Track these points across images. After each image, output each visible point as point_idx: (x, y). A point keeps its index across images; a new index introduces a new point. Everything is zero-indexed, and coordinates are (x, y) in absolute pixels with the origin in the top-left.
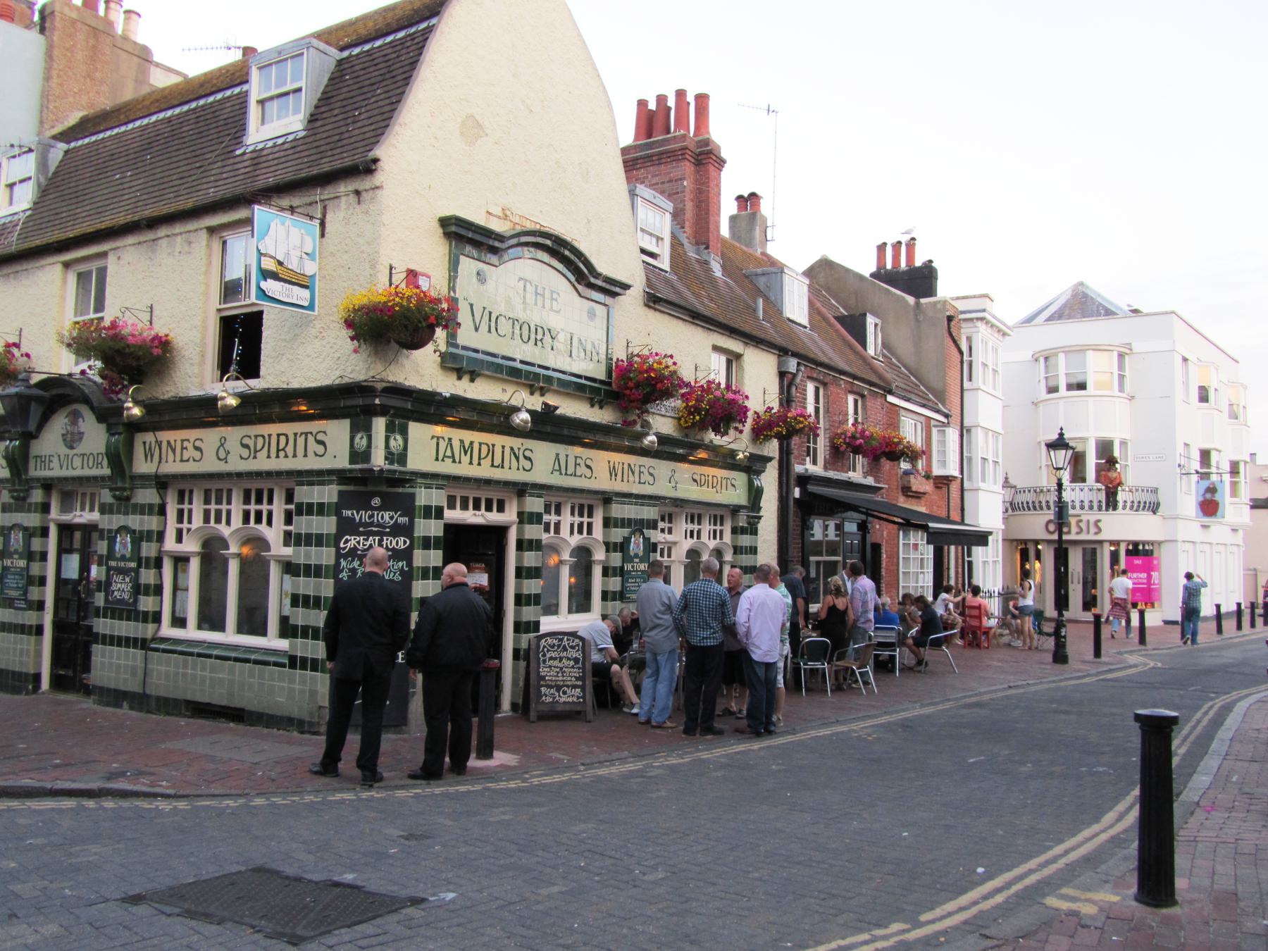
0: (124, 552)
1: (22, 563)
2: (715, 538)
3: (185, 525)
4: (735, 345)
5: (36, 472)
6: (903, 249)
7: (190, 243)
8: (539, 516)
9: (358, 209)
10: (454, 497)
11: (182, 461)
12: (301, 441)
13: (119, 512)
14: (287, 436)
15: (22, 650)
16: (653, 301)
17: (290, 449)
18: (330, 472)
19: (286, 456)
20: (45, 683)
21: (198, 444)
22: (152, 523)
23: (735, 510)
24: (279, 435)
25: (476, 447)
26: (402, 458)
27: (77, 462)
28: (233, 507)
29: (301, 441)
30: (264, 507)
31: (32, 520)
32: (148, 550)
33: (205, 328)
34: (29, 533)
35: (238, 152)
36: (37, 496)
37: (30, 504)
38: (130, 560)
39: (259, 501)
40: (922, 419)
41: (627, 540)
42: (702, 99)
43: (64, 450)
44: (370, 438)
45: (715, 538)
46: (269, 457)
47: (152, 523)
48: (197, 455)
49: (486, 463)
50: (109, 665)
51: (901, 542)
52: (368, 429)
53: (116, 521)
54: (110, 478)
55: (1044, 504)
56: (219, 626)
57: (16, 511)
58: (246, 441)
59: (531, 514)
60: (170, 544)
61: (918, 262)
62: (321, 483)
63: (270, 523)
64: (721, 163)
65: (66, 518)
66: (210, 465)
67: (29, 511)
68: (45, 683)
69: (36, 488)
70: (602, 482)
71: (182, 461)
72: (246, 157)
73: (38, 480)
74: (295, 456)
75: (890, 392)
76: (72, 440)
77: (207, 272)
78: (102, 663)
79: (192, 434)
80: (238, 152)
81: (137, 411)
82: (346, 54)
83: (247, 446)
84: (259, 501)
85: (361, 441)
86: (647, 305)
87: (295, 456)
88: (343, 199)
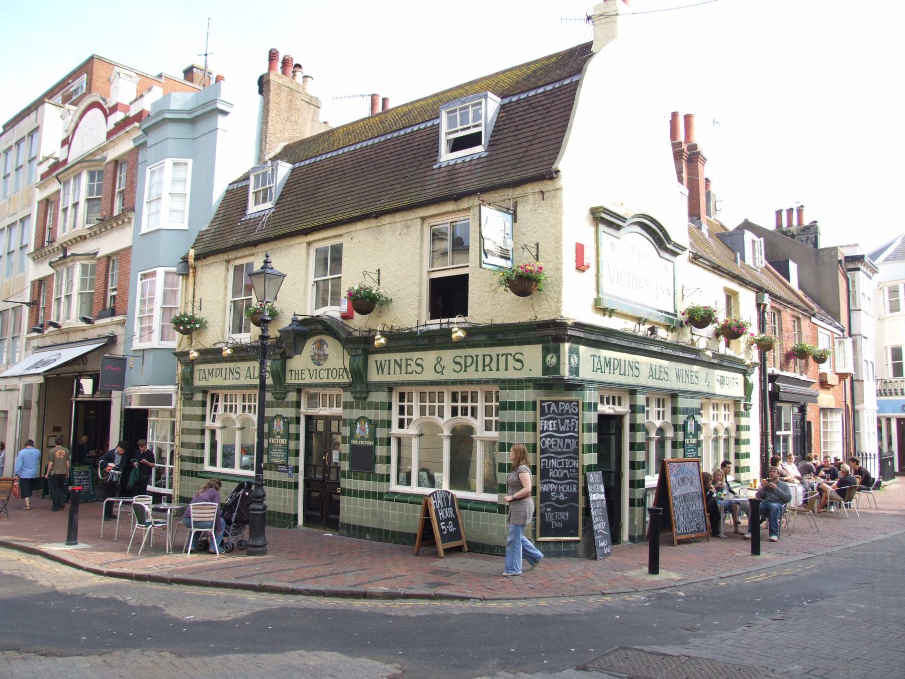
0: (362, 434)
1: (284, 441)
2: (659, 418)
3: (406, 417)
4: (734, 286)
5: (289, 380)
6: (795, 214)
7: (408, 227)
8: (596, 405)
9: (542, 202)
10: (491, 393)
11: (407, 373)
12: (502, 360)
13: (357, 408)
14: (491, 356)
15: (285, 498)
16: (695, 258)
17: (494, 365)
18: (529, 380)
19: (491, 370)
20: (300, 521)
21: (419, 362)
22: (382, 415)
23: (737, 402)
24: (484, 356)
25: (612, 361)
26: (575, 370)
27: (324, 374)
28: (445, 404)
29: (502, 360)
30: (469, 404)
31: (290, 413)
32: (381, 433)
33: (421, 284)
34: (287, 422)
35: (435, 167)
36: (292, 397)
37: (288, 402)
38: (367, 440)
39: (464, 399)
40: (829, 333)
41: (686, 423)
42: (688, 118)
43: (313, 366)
44: (558, 358)
45: (659, 418)
46: (477, 370)
47: (382, 415)
48: (419, 369)
49: (617, 372)
50: (351, 510)
51: (822, 420)
52: (557, 351)
53: (356, 414)
54: (351, 385)
55: (893, 392)
56: (408, 483)
57: (277, 407)
58: (457, 360)
59: (590, 404)
60: (395, 429)
61: (806, 222)
62: (522, 388)
63: (441, 415)
64: (704, 160)
65: (312, 412)
66: (429, 375)
67: (287, 406)
68: (300, 521)
69: (293, 391)
70: (673, 384)
71: (407, 373)
72: (442, 170)
73: (294, 385)
74: (498, 370)
75: (814, 315)
76: (319, 359)
77: (421, 247)
78: (349, 509)
79: (416, 355)
80: (435, 167)
81: (383, 341)
82: (506, 101)
83: (459, 363)
84: (464, 399)
85: (551, 360)
86: (691, 261)
87: (498, 370)
88: (530, 197)
